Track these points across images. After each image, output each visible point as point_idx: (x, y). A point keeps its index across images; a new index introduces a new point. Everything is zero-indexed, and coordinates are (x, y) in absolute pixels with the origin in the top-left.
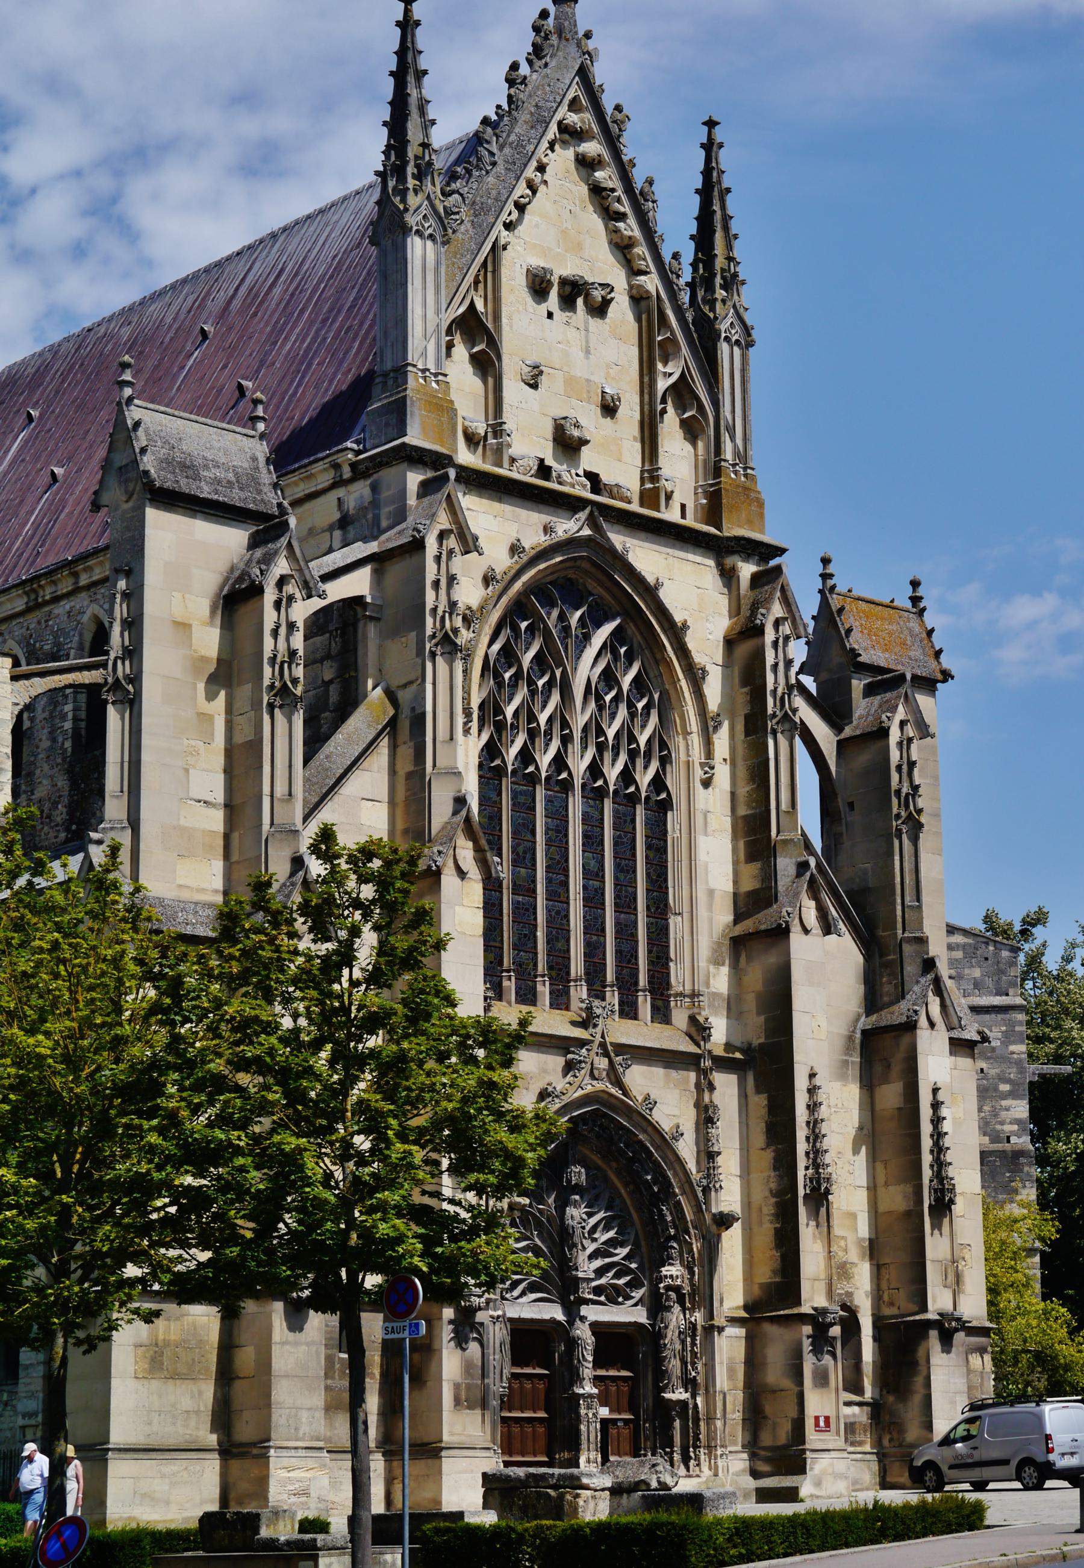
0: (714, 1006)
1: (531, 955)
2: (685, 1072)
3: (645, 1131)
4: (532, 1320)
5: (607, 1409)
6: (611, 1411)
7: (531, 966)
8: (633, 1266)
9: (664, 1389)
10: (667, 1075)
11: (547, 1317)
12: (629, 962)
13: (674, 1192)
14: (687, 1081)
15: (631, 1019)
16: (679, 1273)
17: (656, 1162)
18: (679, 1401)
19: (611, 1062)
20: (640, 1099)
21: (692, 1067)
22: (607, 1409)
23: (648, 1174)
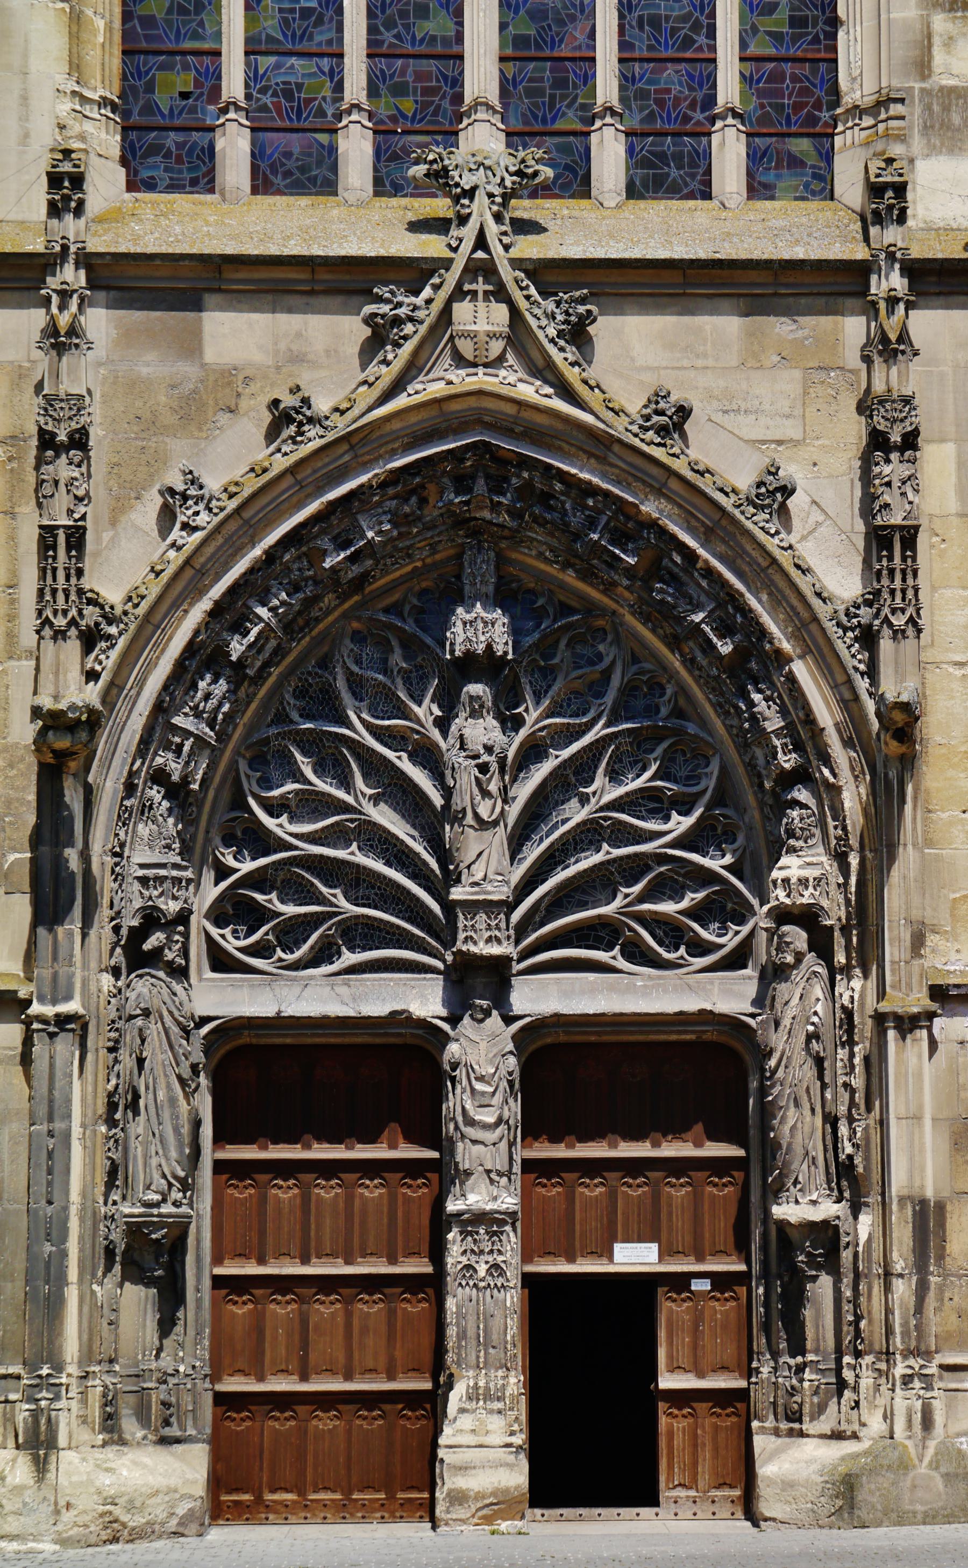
0: (946, 126)
1: (325, 63)
2: (825, 321)
3: (660, 492)
4: (325, 1023)
5: (654, 1247)
6: (663, 1256)
7: (327, 92)
8: (715, 863)
9: (775, 1192)
10: (750, 334)
11: (377, 1008)
12: (688, 42)
13: (778, 652)
14: (836, 342)
15: (691, 196)
16: (811, 873)
17: (709, 572)
18: (811, 1227)
19: (515, 312)
20: (634, 404)
21: (850, 302)
22: (654, 1247)
23: (697, 608)
